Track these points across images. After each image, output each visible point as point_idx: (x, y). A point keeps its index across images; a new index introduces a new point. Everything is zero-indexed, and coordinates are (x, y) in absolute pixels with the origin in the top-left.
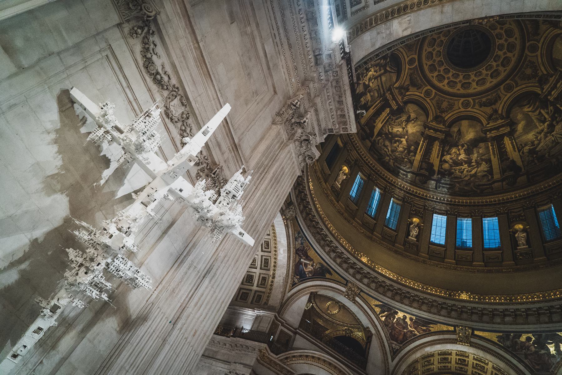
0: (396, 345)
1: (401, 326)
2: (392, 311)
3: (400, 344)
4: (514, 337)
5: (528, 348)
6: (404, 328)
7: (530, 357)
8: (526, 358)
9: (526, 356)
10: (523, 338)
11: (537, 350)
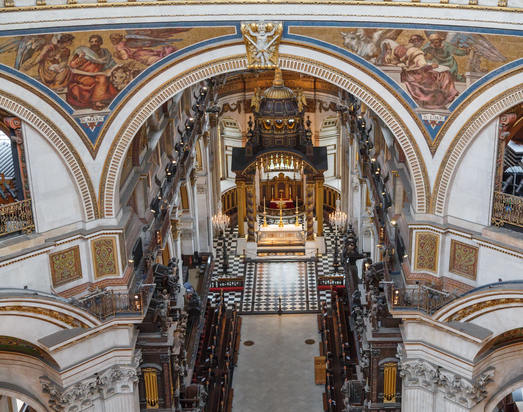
0: (92, 115)
1: (90, 67)
2: (54, 41)
3: (102, 108)
4: (382, 38)
5: (411, 60)
6: (101, 67)
7: (411, 78)
8: (402, 80)
9: (404, 75)
10: (403, 39)
11: (430, 64)
